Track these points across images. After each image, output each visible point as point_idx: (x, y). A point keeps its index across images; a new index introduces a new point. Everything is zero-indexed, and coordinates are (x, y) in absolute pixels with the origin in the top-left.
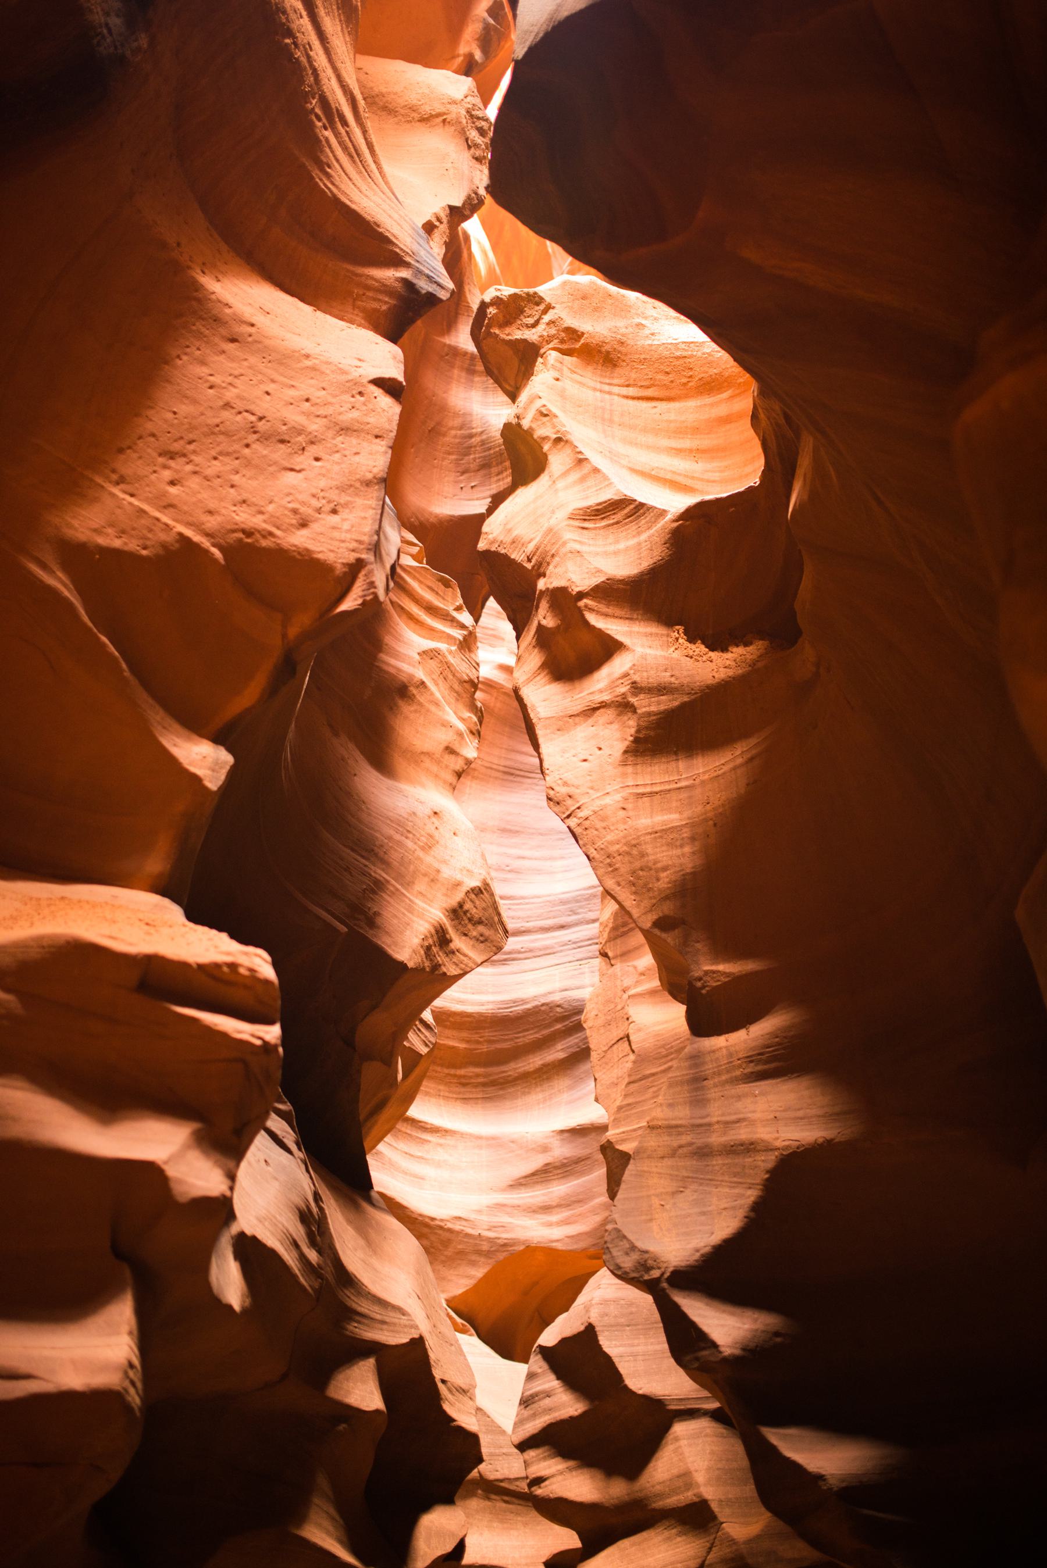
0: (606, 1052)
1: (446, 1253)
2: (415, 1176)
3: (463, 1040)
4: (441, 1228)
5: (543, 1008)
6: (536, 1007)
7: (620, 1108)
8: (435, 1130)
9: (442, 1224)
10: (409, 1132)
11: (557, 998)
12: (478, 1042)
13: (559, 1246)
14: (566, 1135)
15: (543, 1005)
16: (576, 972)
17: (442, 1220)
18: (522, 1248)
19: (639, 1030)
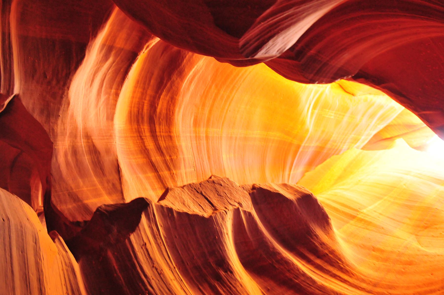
0: (201, 194)
1: (48, 96)
2: (93, 81)
3: (161, 110)
4: (63, 93)
5: (176, 150)
6: (176, 146)
7: (170, 210)
8: (117, 95)
9: (65, 94)
10: (117, 80)
11: (181, 156)
12: (159, 118)
13: (54, 160)
14: (116, 163)
15: (177, 149)
16: (191, 165)
17: (68, 93)
18: (52, 140)
19: (223, 219)
